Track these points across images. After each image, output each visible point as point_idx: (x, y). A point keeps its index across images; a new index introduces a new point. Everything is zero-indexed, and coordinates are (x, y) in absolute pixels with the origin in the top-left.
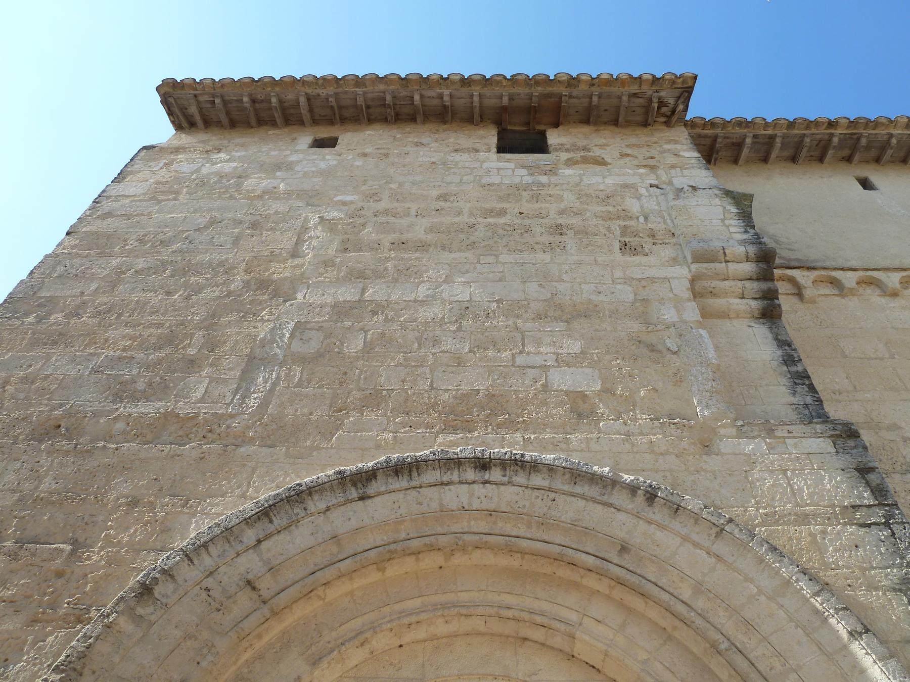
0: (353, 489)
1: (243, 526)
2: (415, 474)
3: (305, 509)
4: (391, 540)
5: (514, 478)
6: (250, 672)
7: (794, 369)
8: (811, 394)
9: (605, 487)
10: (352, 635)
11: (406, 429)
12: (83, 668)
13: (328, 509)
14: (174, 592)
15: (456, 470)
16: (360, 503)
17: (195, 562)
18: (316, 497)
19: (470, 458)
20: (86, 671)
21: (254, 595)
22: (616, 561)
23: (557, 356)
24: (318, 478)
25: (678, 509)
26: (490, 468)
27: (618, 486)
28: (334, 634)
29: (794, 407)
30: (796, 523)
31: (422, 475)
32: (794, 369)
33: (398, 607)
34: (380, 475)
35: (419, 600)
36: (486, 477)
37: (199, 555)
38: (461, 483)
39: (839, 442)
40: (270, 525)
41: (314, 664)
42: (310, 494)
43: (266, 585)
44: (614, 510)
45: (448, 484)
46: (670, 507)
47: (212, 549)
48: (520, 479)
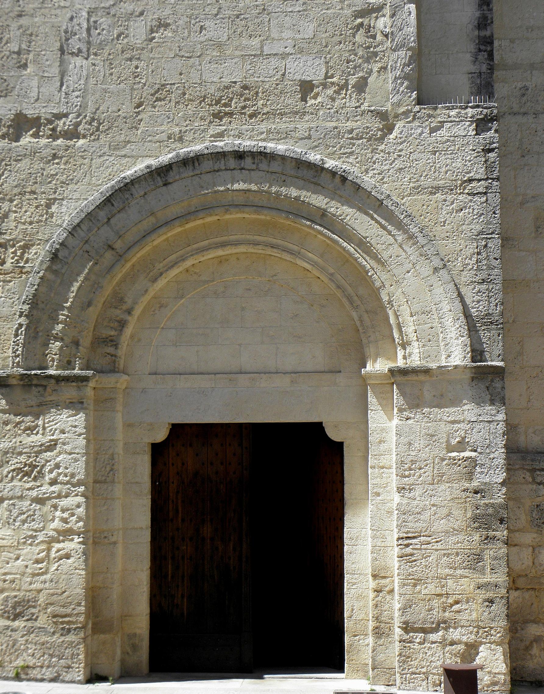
0: (159, 178)
1: (97, 210)
2: (196, 164)
3: (132, 194)
4: (187, 212)
5: (260, 165)
6: (120, 289)
7: (483, 33)
8: (488, 62)
9: (317, 171)
10: (171, 264)
11: (187, 122)
12: (37, 301)
13: (145, 194)
14: (70, 254)
15: (223, 159)
16: (164, 188)
17: (76, 235)
18: (137, 186)
19: (230, 152)
20: (39, 302)
21: (113, 253)
22: (319, 222)
23: (295, 42)
24: (136, 172)
25: (359, 188)
26: (244, 158)
27: (324, 171)
28: (161, 265)
29: (470, 76)
30: (431, 193)
31: (201, 165)
32: (483, 33)
33: (195, 246)
34: (174, 167)
35: (207, 241)
36: (242, 165)
37: (76, 231)
38: (226, 169)
39: (481, 125)
40: (112, 208)
41: (153, 282)
42: (133, 184)
43: (118, 245)
44: (321, 188)
45: (218, 171)
46: (354, 187)
47: (82, 226)
48: (263, 166)
